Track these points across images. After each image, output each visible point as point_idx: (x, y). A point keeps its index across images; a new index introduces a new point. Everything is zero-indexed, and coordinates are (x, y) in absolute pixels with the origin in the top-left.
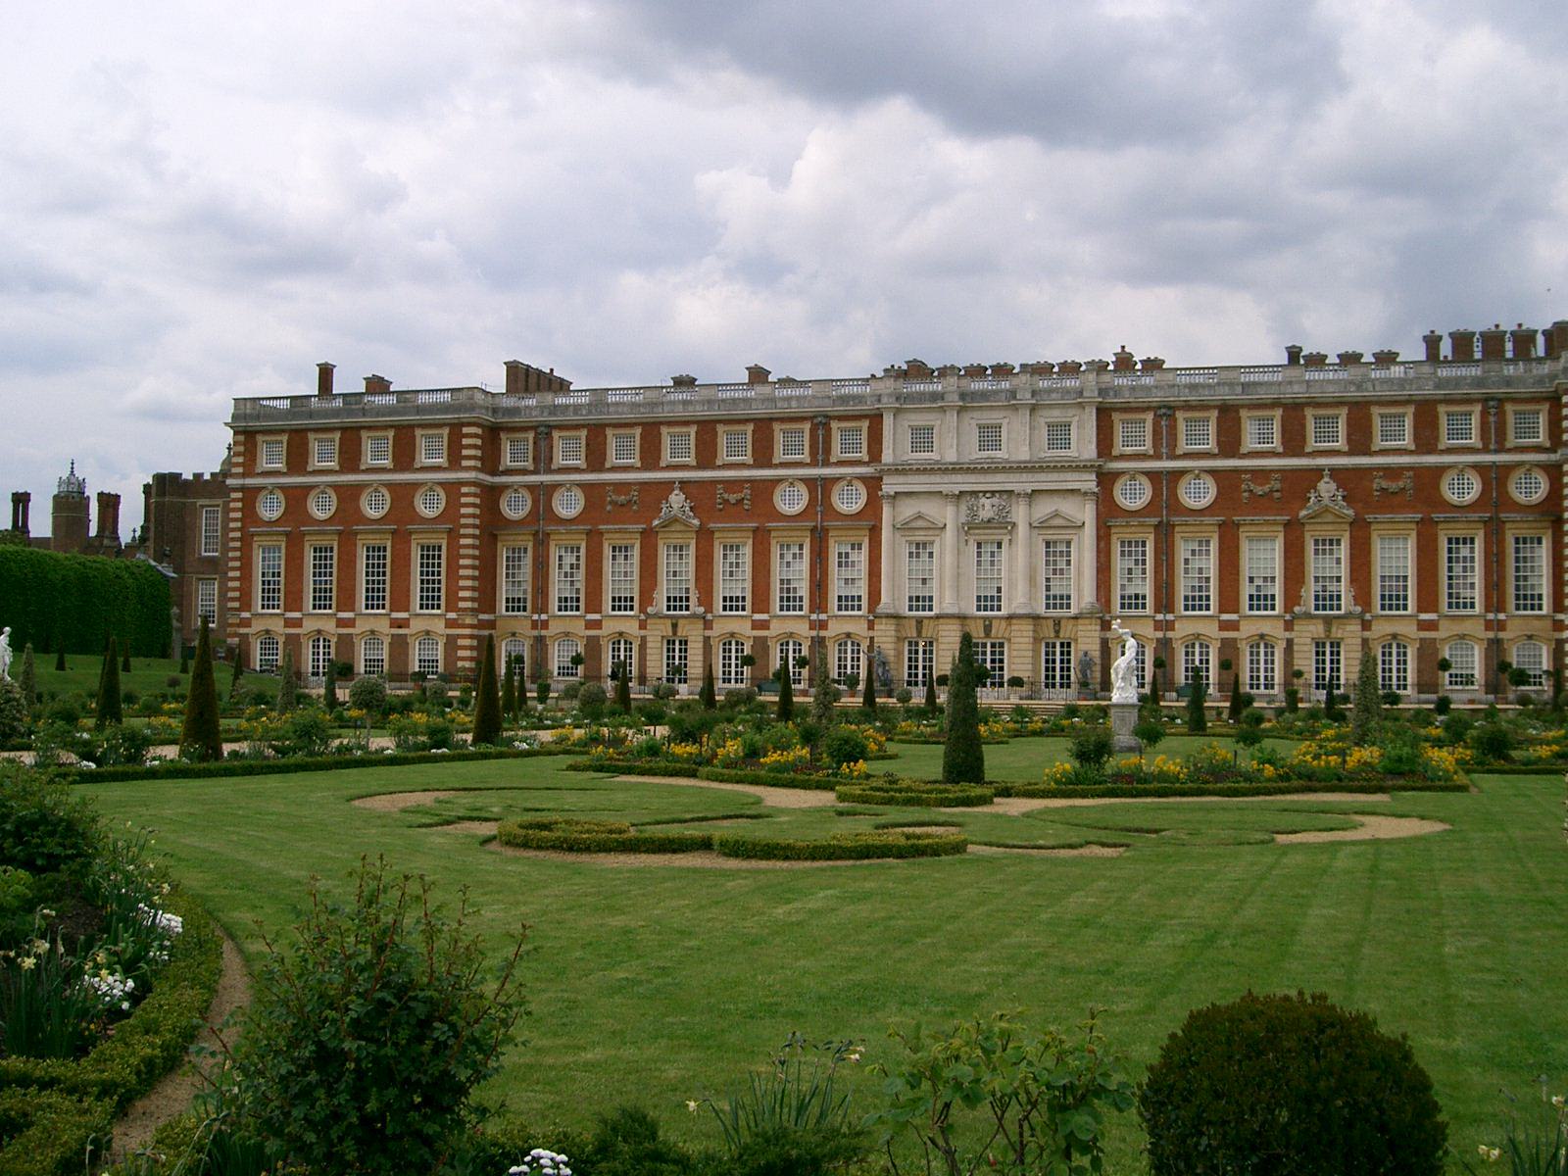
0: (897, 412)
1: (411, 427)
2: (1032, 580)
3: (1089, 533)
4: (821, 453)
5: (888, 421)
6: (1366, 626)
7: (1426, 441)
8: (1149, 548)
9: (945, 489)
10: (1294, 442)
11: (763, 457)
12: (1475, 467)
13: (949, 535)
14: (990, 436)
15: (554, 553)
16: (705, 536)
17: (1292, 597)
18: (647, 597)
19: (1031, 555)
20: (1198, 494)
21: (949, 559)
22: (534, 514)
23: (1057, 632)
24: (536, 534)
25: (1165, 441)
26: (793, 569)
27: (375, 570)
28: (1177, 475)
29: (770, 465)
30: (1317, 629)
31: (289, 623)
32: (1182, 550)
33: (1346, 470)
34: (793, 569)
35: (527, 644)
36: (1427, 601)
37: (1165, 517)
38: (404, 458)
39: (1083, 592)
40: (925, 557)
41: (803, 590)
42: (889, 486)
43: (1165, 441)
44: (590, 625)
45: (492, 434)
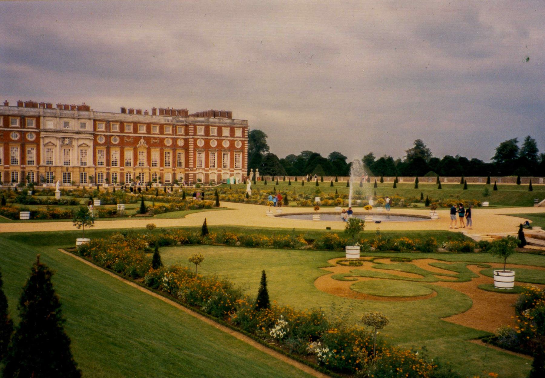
0: (44, 117)
2: (78, 159)
3: (92, 148)
5: (42, 118)
7: (162, 132)
9: (57, 136)
10: (135, 131)
13: (58, 147)
14: (66, 124)
17: (135, 164)
19: (78, 152)
20: (116, 141)
23: (84, 171)
29: (8, 127)
32: (112, 152)
34: (16, 154)
39: (90, 162)
40: (50, 152)
42: (42, 135)
43: (108, 128)
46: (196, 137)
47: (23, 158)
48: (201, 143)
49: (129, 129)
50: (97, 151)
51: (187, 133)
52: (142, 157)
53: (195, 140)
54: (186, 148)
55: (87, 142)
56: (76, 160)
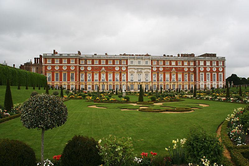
1: (70, 58)
4: (120, 63)
5: (128, 60)
6: (177, 83)
7: (183, 64)
8: (156, 75)
11: (114, 64)
12: (187, 67)
14: (139, 62)
15: (88, 74)
16: (107, 73)
17: (170, 80)
18: (100, 80)
20: (161, 69)
21: (136, 76)
22: (85, 70)
24: (85, 72)
25: (158, 64)
26: (117, 77)
27: (65, 76)
28: (159, 67)
30: (173, 83)
31: (52, 83)
32: (160, 75)
33: (175, 67)
34: (117, 77)
35: (84, 86)
36: (183, 81)
37: (158, 71)
38: (69, 62)
39: (150, 80)
40: (132, 75)
41: (119, 79)
43: (158, 64)
44: (92, 83)
45: (80, 59)
46: (199, 66)
47: (121, 79)
48: (202, 69)
49: (167, 63)
50: (153, 75)
51: (195, 64)
52: (174, 77)
53: (199, 68)
54: (195, 72)
55: (148, 70)
56: (144, 79)
